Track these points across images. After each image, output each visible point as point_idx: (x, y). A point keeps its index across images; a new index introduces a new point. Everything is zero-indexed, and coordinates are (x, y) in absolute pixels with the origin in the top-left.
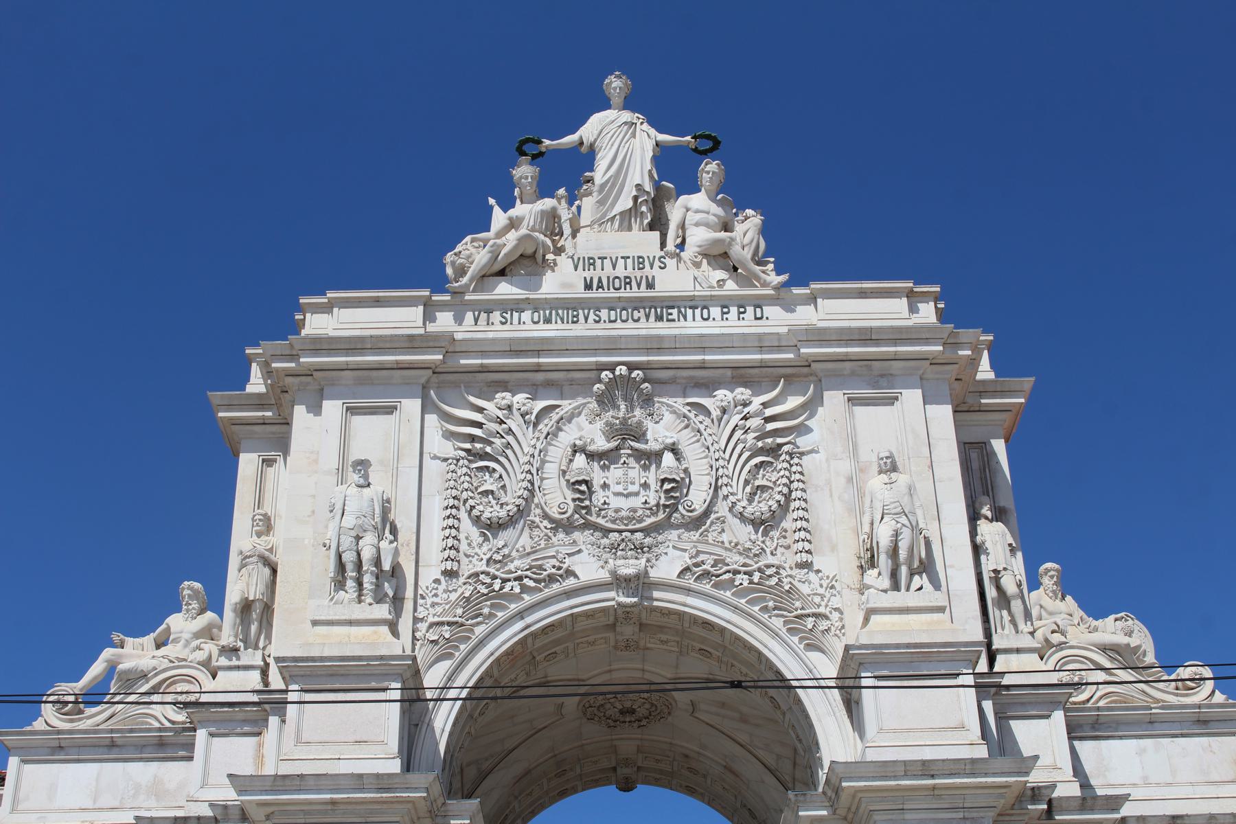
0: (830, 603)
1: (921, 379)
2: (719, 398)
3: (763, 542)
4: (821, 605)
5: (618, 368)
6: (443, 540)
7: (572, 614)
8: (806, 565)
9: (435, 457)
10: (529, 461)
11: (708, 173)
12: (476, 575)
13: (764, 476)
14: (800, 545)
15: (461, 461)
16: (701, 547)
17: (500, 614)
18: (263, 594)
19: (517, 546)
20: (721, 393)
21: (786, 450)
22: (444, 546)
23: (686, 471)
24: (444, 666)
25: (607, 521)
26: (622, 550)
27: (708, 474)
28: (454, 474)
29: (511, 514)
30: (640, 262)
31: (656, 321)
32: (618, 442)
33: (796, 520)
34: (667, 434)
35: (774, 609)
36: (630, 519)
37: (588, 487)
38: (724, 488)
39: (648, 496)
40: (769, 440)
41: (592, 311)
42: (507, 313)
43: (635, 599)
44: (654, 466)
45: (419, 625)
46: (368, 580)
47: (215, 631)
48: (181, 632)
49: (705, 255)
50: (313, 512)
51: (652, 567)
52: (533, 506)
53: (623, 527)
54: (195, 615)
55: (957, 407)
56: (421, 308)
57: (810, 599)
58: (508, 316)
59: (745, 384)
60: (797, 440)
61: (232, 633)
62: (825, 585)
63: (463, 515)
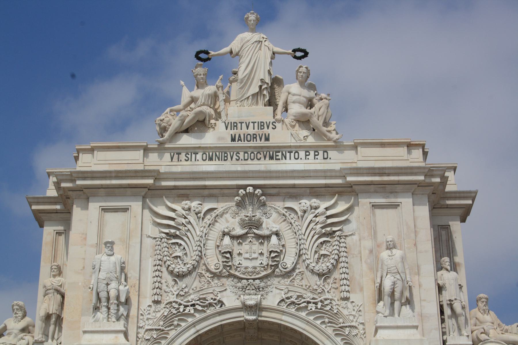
0: (358, 320)
1: (413, 194)
2: (303, 204)
3: (324, 286)
4: (353, 321)
5: (248, 188)
6: (153, 283)
7: (221, 325)
8: (347, 299)
9: (149, 237)
10: (200, 240)
11: (301, 72)
12: (171, 303)
13: (325, 248)
15: (163, 240)
16: (291, 288)
17: (183, 324)
18: (57, 310)
19: (192, 287)
20: (303, 201)
21: (337, 235)
22: (154, 287)
23: (283, 246)
25: (241, 274)
26: (249, 290)
27: (295, 248)
28: (159, 247)
29: (189, 269)
30: (261, 125)
31: (269, 159)
32: (246, 231)
33: (342, 274)
34: (274, 225)
35: (329, 322)
36: (253, 272)
37: (231, 255)
38: (303, 256)
39: (263, 260)
40: (328, 229)
41: (235, 153)
42: (189, 155)
43: (254, 317)
44: (266, 242)
45: (140, 330)
46: (113, 307)
47: (30, 328)
48: (13, 329)
49: (298, 121)
50: (84, 267)
51: (264, 299)
52: (201, 265)
53: (249, 277)
54: (20, 320)
55: (434, 205)
56: (142, 151)
57: (347, 317)
58: (189, 156)
60: (343, 227)
61: (40, 332)
62: (356, 310)
63: (164, 269)
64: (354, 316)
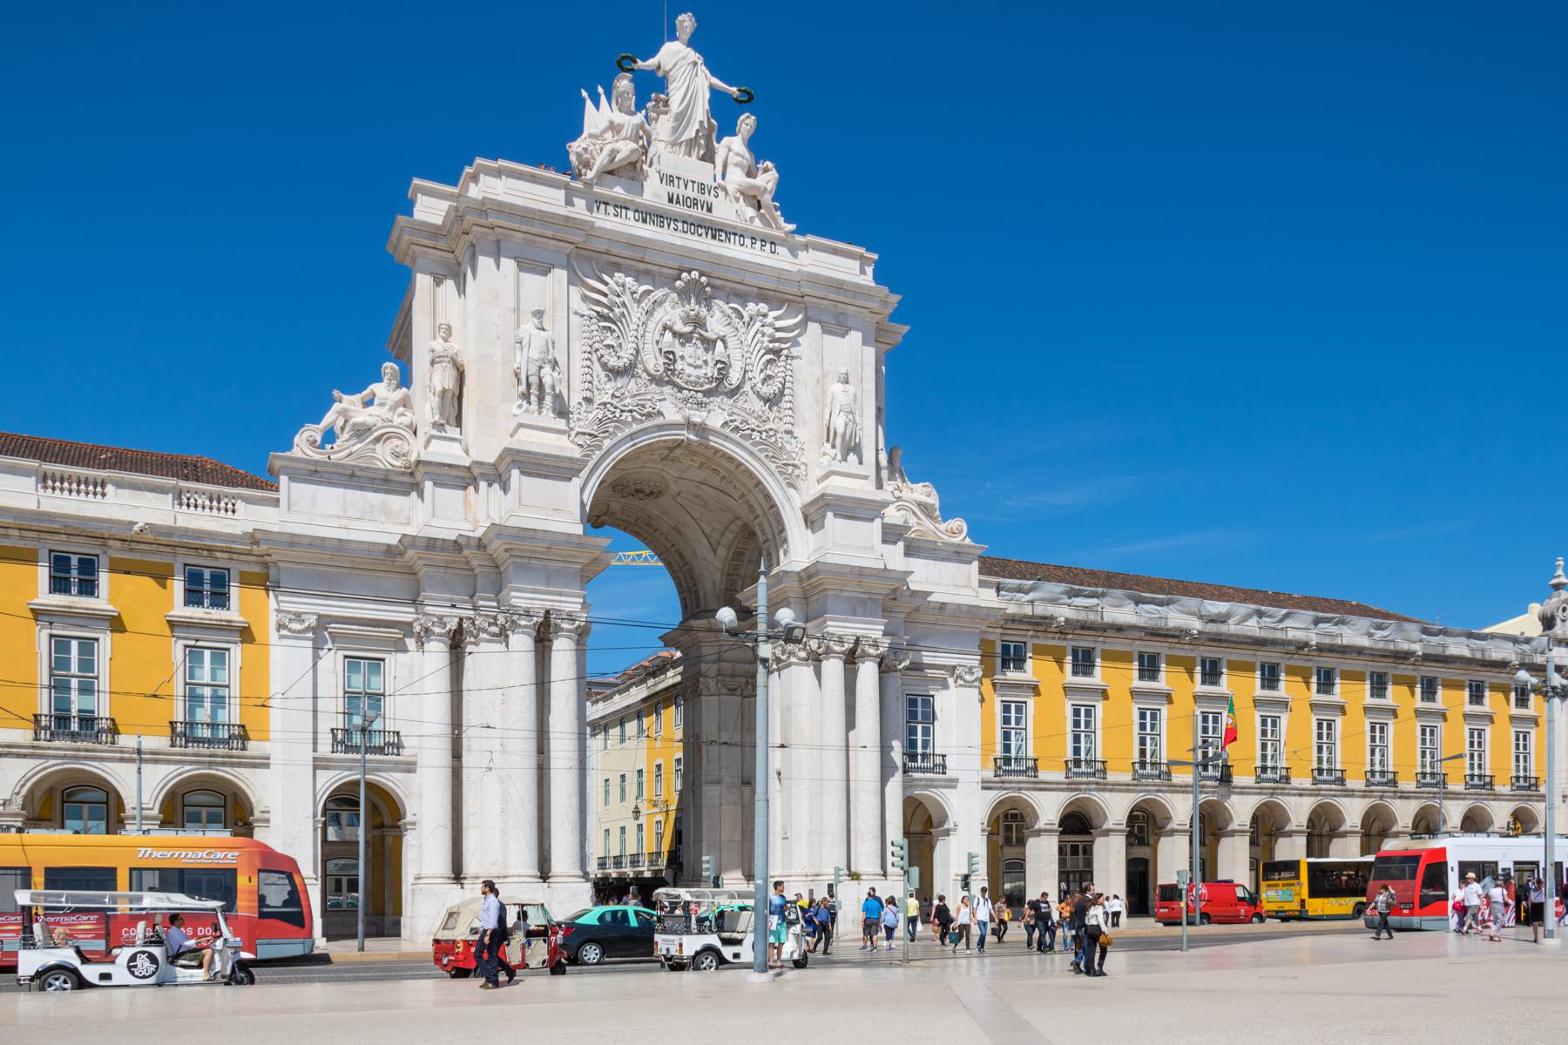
11: (747, 125)
14: (789, 419)
16: (735, 410)
30: (702, 188)
36: (696, 383)
40: (777, 345)
49: (742, 193)
59: (764, 299)
64: (797, 454)
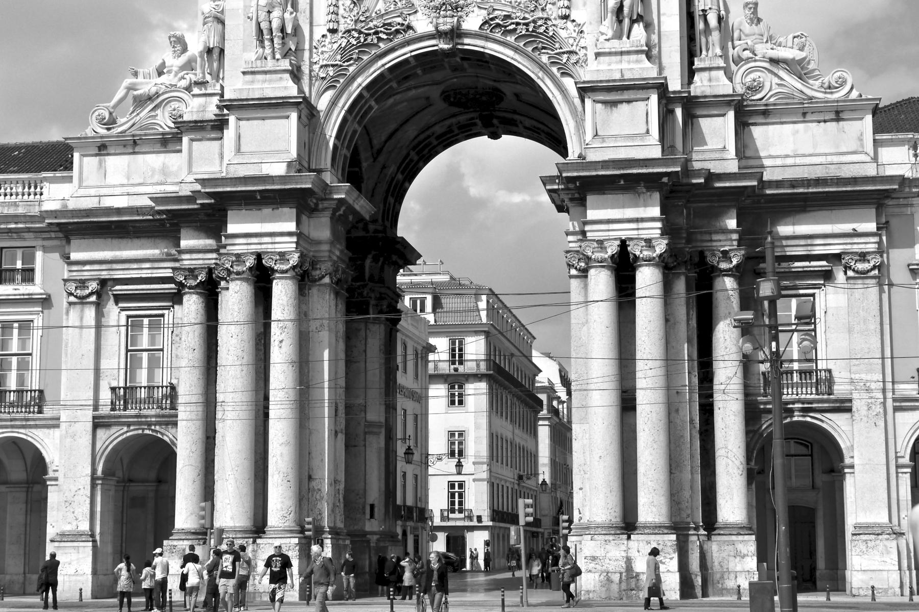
8: (566, 17)
12: (349, 31)
17: (365, 58)
24: (329, 95)
43: (450, 46)
47: (193, 64)
48: (172, 66)
57: (566, 41)
62: (577, 31)
